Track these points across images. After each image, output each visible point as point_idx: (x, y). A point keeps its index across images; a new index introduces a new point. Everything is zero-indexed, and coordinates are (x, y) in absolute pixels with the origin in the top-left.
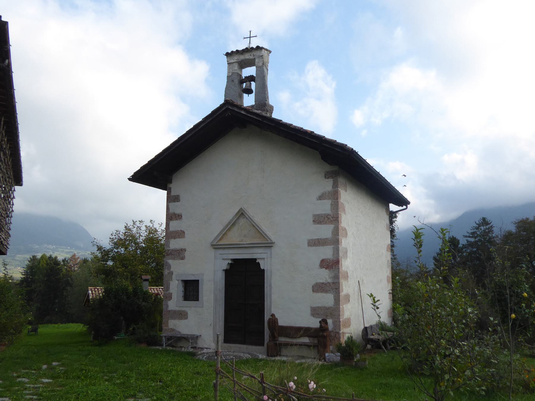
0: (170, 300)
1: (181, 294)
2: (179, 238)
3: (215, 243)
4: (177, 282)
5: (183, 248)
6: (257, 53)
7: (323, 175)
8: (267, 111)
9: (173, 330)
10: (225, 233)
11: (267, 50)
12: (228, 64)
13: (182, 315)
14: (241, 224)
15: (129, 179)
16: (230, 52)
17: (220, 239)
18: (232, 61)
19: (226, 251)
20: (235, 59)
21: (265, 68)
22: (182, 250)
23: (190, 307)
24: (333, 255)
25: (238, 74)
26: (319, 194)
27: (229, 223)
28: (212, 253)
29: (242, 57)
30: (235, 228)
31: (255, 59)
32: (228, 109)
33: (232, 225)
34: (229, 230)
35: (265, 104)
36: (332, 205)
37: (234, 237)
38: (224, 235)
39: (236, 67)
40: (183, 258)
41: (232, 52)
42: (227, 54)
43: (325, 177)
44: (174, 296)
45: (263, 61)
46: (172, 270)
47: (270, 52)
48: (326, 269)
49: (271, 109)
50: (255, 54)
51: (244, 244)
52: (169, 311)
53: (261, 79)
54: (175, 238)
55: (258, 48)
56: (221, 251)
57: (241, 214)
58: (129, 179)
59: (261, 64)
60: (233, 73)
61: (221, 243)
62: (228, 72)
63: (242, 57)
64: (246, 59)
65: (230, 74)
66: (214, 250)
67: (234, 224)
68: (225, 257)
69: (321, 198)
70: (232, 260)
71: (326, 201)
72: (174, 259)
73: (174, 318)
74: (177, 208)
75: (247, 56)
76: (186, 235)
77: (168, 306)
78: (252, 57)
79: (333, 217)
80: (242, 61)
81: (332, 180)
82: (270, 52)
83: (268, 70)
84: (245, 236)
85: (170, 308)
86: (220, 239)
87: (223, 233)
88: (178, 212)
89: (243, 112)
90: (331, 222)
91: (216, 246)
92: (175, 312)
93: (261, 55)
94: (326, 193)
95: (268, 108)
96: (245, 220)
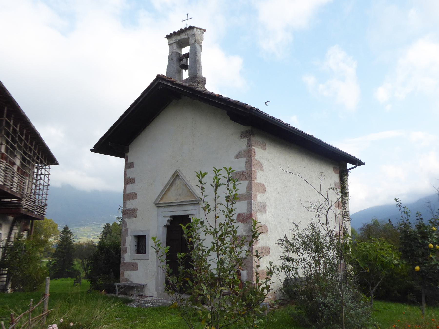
0: (125, 253)
1: (135, 248)
2: (133, 199)
3: (157, 203)
4: (131, 237)
5: (136, 207)
6: (190, 32)
7: (239, 135)
8: (198, 82)
9: (127, 280)
10: (165, 193)
11: (200, 29)
12: (169, 45)
13: (134, 267)
14: (177, 185)
15: (92, 150)
16: (169, 34)
17: (162, 199)
18: (172, 42)
19: (166, 209)
20: (174, 39)
21: (197, 45)
22: (134, 209)
23: (139, 260)
24: (247, 209)
25: (176, 53)
26: (236, 153)
27: (168, 184)
28: (155, 211)
29: (179, 38)
30: (173, 188)
31: (189, 38)
32: (159, 83)
33: (170, 185)
34: (168, 190)
35: (196, 76)
36: (246, 162)
37: (172, 197)
38: (164, 194)
39: (175, 46)
40: (135, 217)
41: (171, 34)
42: (168, 37)
43: (241, 137)
44: (129, 250)
45: (195, 38)
46: (127, 227)
47: (205, 31)
48: (242, 222)
49: (204, 81)
51: (178, 202)
52: (125, 263)
53: (194, 56)
54: (130, 199)
55: (191, 28)
56: (162, 210)
57: (176, 176)
58: (92, 150)
59: (193, 42)
60: (173, 52)
61: (161, 202)
62: (169, 52)
63: (179, 38)
64: (182, 39)
65: (171, 54)
66: (157, 208)
67: (172, 185)
68: (166, 214)
69: (237, 157)
70: (171, 217)
71: (242, 159)
72: (129, 217)
73: (128, 269)
74: (132, 174)
75: (183, 36)
76: (138, 197)
77: (124, 259)
78: (186, 37)
79: (247, 174)
80: (179, 40)
81: (246, 139)
82: (205, 31)
83: (201, 46)
84: (180, 195)
85: (126, 261)
86: (162, 199)
87: (163, 193)
88: (132, 177)
89: (169, 84)
90: (245, 179)
91: (159, 205)
92: (129, 264)
93: (193, 33)
94: (241, 152)
95: (200, 80)
96: (180, 180)
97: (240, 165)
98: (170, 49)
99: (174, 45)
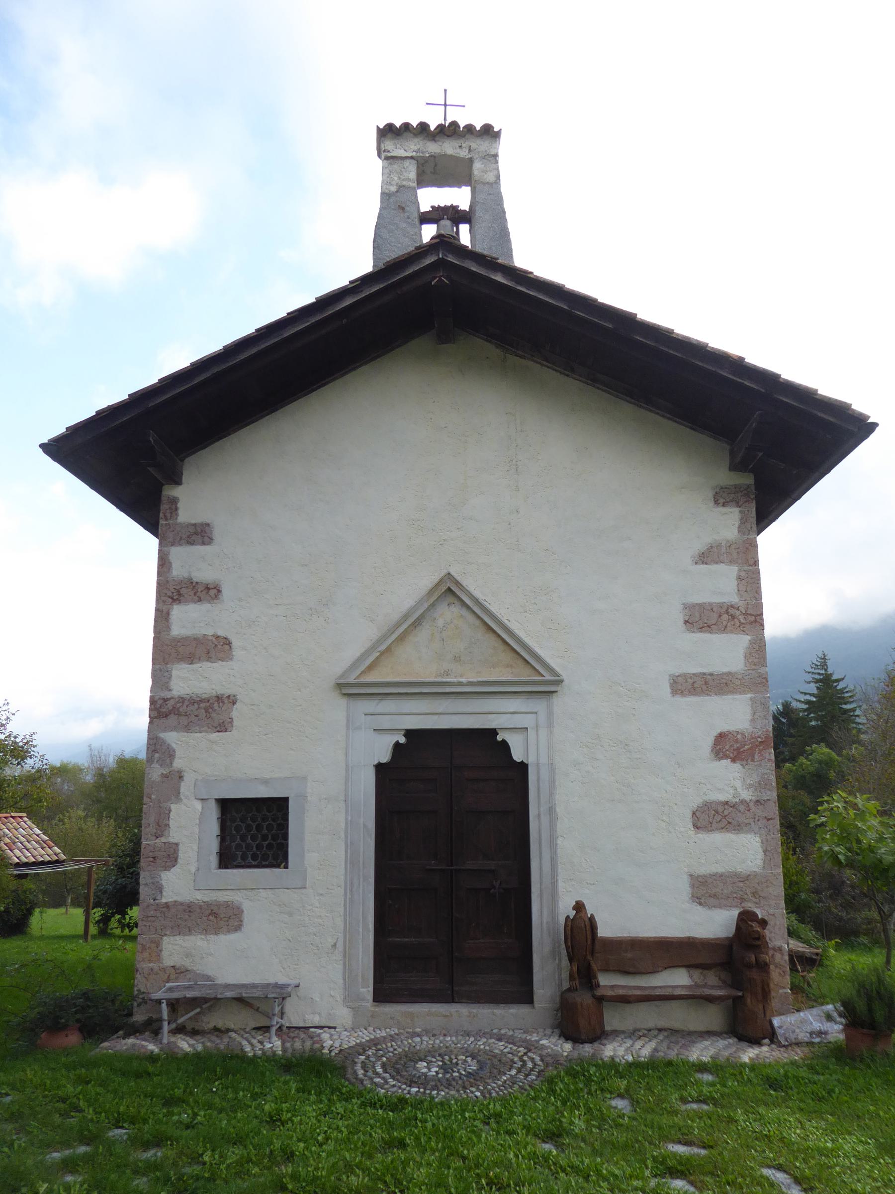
0: (167, 868)
1: (213, 845)
2: (209, 659)
3: (351, 679)
4: (198, 806)
5: (226, 691)
6: (481, 145)
7: (711, 494)
9: (179, 972)
10: (388, 650)
13: (221, 918)
14: (440, 622)
15: (42, 446)
17: (370, 668)
18: (401, 153)
19: (389, 705)
20: (410, 147)
22: (219, 698)
23: (247, 886)
24: (753, 720)
26: (699, 546)
27: (406, 617)
28: (338, 709)
29: (432, 148)
30: (422, 635)
31: (471, 161)
33: (413, 622)
34: (402, 638)
36: (739, 578)
37: (418, 661)
38: (382, 653)
40: (223, 727)
41: (406, 126)
42: (388, 132)
43: (716, 502)
44: (188, 854)
46: (178, 764)
48: (734, 760)
50: (474, 145)
51: (460, 684)
52: (167, 905)
54: (191, 659)
56: (370, 706)
57: (449, 591)
58: (42, 446)
61: (370, 678)
63: (432, 148)
65: (393, 189)
66: (343, 702)
67: (417, 623)
68: (386, 722)
69: (705, 557)
70: (409, 733)
71: (722, 567)
72: (187, 728)
73: (180, 929)
74: (192, 562)
75: (449, 147)
76: (237, 652)
77: (160, 889)
78: (463, 153)
79: (746, 614)
81: (737, 510)
84: (457, 659)
85: (168, 897)
86: (370, 668)
87: (383, 647)
88: (204, 574)
90: (741, 628)
91: (350, 690)
92: (189, 908)
94: (719, 546)
96: (456, 610)
97: (719, 585)
98: (387, 174)
99: (407, 163)
